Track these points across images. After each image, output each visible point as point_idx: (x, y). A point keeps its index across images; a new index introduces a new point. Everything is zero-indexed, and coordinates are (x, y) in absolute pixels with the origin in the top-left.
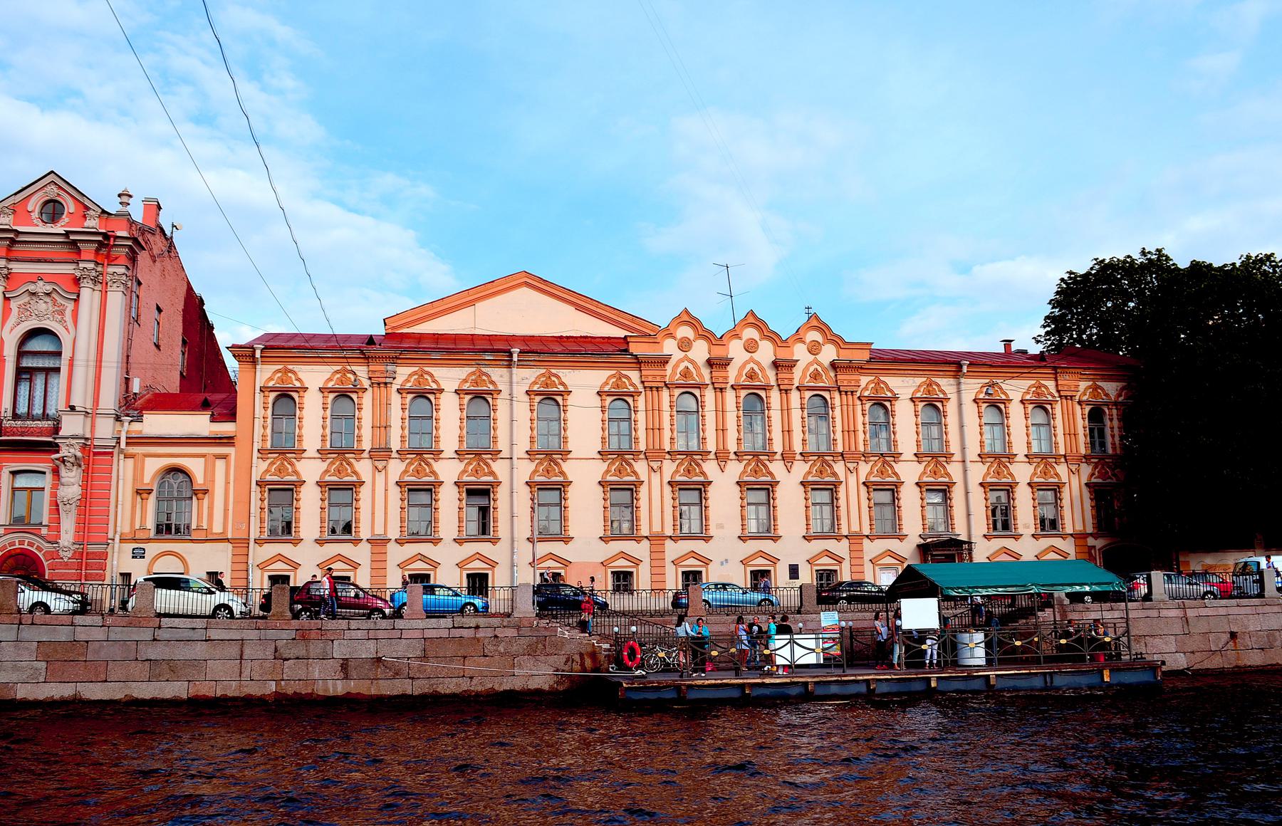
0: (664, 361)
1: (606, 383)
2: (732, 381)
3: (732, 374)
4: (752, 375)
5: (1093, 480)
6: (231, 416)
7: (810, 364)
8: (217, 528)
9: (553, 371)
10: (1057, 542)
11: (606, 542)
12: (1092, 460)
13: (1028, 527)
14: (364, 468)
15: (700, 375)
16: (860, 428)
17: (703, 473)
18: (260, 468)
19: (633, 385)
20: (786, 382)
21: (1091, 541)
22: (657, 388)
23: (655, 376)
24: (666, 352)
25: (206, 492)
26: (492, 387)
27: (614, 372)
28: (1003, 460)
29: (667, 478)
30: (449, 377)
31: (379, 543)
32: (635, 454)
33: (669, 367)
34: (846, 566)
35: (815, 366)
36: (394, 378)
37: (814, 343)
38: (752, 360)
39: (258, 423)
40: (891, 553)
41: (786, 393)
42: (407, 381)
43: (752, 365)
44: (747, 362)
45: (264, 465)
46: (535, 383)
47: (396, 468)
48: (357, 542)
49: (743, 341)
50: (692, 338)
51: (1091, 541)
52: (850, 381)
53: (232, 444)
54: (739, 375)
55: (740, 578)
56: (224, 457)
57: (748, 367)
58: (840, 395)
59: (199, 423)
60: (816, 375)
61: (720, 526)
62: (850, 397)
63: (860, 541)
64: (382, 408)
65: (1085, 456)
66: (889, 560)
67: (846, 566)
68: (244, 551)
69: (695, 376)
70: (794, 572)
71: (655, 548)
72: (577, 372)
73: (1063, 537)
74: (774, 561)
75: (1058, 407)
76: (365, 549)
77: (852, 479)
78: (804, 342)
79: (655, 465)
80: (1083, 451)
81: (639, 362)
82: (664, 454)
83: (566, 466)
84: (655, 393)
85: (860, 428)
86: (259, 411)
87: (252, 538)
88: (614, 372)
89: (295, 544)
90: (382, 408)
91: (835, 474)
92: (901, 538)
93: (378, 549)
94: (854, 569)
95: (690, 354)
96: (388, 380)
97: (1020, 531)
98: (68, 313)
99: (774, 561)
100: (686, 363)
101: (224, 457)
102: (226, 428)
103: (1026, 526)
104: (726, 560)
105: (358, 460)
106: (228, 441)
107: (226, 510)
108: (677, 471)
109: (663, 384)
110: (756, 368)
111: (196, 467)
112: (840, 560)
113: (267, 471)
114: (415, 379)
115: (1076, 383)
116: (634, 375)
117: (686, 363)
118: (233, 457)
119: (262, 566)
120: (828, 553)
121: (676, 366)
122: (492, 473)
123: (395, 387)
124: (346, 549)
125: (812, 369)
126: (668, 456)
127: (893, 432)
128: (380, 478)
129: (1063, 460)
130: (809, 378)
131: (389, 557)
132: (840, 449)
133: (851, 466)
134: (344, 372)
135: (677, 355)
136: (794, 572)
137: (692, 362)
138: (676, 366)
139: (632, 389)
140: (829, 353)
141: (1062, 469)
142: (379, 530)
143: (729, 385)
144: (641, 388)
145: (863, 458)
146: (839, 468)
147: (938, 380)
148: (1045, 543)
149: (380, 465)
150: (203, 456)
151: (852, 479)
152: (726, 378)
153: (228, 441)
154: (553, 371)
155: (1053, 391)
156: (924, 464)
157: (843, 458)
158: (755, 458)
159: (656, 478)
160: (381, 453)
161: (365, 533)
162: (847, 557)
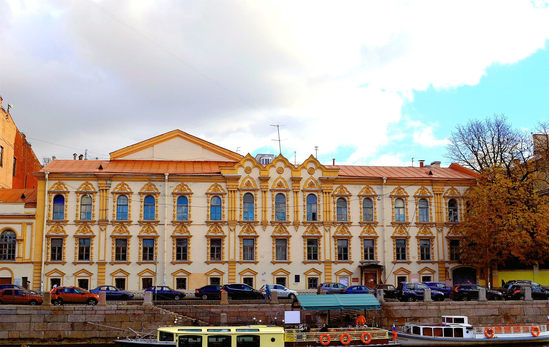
0: (237, 179)
2: (270, 188)
3: (270, 184)
4: (280, 185)
5: (450, 235)
6: (34, 204)
7: (309, 179)
8: (27, 257)
9: (185, 183)
10: (430, 266)
11: (208, 264)
12: (449, 225)
13: (415, 258)
14: (95, 229)
15: (255, 185)
16: (332, 210)
17: (255, 232)
18: (47, 229)
19: (222, 189)
20: (296, 188)
21: (447, 265)
22: (234, 191)
23: (233, 186)
24: (239, 174)
25: (22, 240)
26: (156, 191)
27: (214, 183)
28: (404, 225)
30: (136, 187)
31: (102, 264)
32: (223, 223)
33: (240, 181)
35: (311, 180)
36: (110, 187)
37: (311, 169)
38: (280, 177)
39: (46, 208)
40: (344, 270)
41: (296, 193)
42: (116, 188)
43: (280, 180)
44: (278, 178)
45: (49, 228)
46: (176, 189)
47: (110, 229)
48: (91, 263)
49: (276, 168)
51: (447, 265)
52: (327, 187)
53: (35, 218)
54: (274, 184)
55: (271, 282)
56: (31, 224)
57: (278, 181)
58: (323, 194)
59: (20, 209)
60: (312, 185)
61: (262, 257)
62: (328, 195)
63: (330, 264)
65: (445, 223)
66: (344, 274)
67: (322, 276)
68: (39, 268)
69: (252, 185)
70: (297, 279)
71: (231, 267)
72: (196, 183)
73: (433, 263)
74: (288, 273)
75: (433, 200)
77: (327, 235)
78: (306, 169)
79: (232, 228)
80: (445, 221)
81: (226, 179)
82: (236, 223)
84: (233, 193)
85: (332, 210)
86: (47, 203)
87: (43, 261)
88: (214, 183)
89: (63, 265)
91: (319, 232)
93: (101, 267)
94: (327, 277)
95: (250, 175)
96: (107, 188)
97: (411, 260)
99: (288, 273)
100: (248, 179)
101: (31, 224)
102: (31, 211)
104: (265, 273)
105: (92, 225)
106: (32, 217)
107: (31, 249)
108: (242, 231)
109: (237, 190)
110: (282, 181)
111: (17, 229)
112: (320, 273)
113: (50, 230)
114: (120, 187)
115: (442, 187)
116: (223, 185)
117: (248, 179)
118: (34, 225)
119: (47, 275)
120: (314, 270)
121: (244, 180)
122: (155, 232)
123: (111, 190)
124: (87, 267)
125: (309, 181)
126: (238, 224)
127: (349, 212)
128: (103, 233)
129: (434, 225)
130: (308, 186)
131: (106, 270)
132: (321, 220)
136: (297, 279)
137: (251, 178)
138: (244, 180)
139: (222, 191)
140: (318, 174)
141: (434, 230)
142: (102, 258)
143: (269, 189)
144: (227, 192)
145: (333, 224)
146: (321, 229)
147: (372, 186)
148: (423, 266)
149: (103, 228)
150: (21, 224)
151: (327, 235)
152: (267, 186)
153: (32, 217)
154: (185, 183)
158: (280, 225)
159: (232, 234)
160: (103, 222)
162: (323, 272)
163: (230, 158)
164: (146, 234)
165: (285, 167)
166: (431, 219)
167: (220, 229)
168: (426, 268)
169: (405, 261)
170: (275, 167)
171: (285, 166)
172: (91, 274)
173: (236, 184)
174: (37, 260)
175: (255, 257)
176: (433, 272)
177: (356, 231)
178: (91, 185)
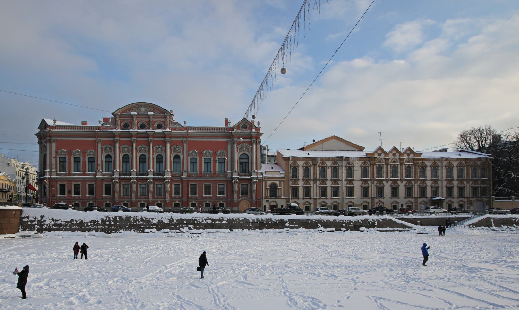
16: (418, 173)
29: (375, 185)
34: (414, 204)
38: (394, 158)
42: (320, 164)
61: (386, 195)
62: (416, 166)
64: (315, 170)
66: (423, 203)
67: (414, 204)
70: (402, 205)
74: (398, 203)
83: (353, 182)
85: (418, 173)
90: (315, 170)
91: (412, 184)
95: (381, 157)
98: (250, 150)
103: (456, 196)
107: (284, 192)
121: (378, 159)
123: (318, 165)
125: (408, 160)
133: (416, 182)
135: (378, 157)
136: (402, 205)
138: (378, 159)
140: (412, 156)
155: (464, 164)
162: (414, 202)
168: (461, 201)
170: (392, 153)
172: (311, 204)
176: (464, 202)
177: (429, 183)
178: (309, 163)
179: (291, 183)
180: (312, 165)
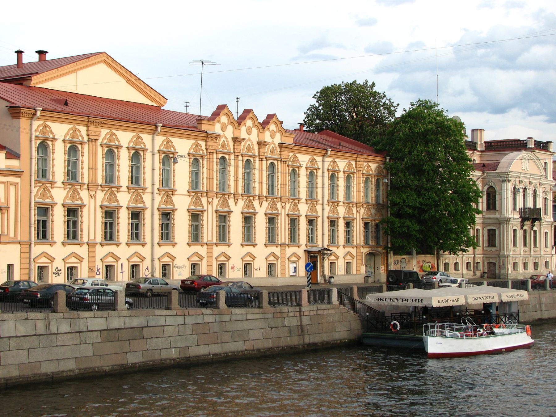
1: (191, 149)
10: (350, 249)
14: (84, 194)
19: (202, 150)
48: (81, 244)
50: (227, 124)
56: (15, 185)
64: (93, 155)
76: (85, 247)
90: (93, 155)
92: (299, 246)
109: (215, 151)
123: (100, 142)
124: (75, 249)
128: (92, 201)
134: (75, 130)
156: (37, 188)
157: (281, 200)
161: (85, 240)
163: (152, 99)
164: (108, 203)
165: (253, 127)
166: (82, 178)
167: (78, 196)
169: (334, 245)
171: (228, 121)
173: (215, 144)
174: (27, 239)
175: (51, 235)
178: (80, 132)
179: (34, 191)
180: (86, 139)
